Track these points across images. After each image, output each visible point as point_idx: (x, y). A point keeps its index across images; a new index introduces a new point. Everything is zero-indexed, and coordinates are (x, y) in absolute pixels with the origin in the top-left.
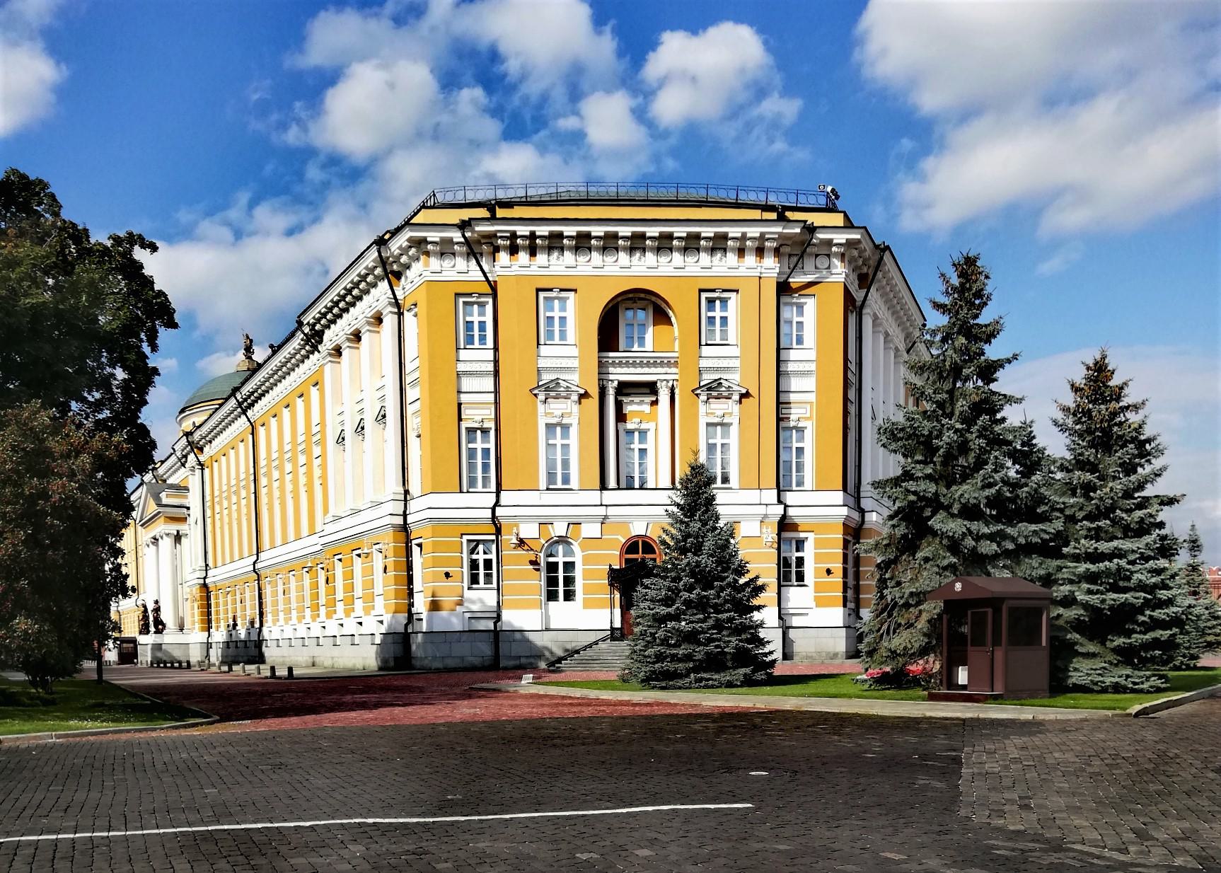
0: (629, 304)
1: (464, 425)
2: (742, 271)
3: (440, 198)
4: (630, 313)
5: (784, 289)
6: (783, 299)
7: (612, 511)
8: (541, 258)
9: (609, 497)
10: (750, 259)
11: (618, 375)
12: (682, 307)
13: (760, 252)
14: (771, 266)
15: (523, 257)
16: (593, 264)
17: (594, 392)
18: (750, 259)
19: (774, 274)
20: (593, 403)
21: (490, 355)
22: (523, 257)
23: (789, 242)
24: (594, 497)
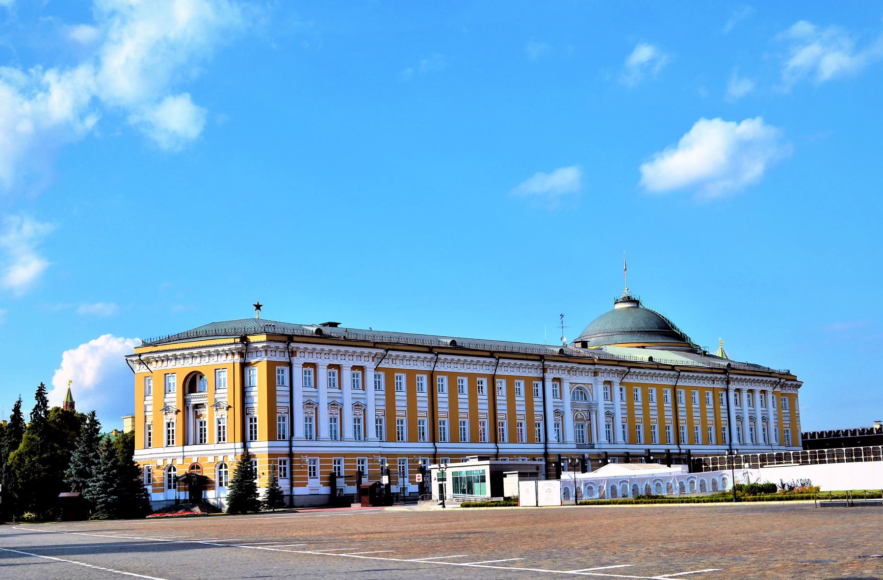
1: (147, 423)
5: (244, 366)
6: (247, 370)
7: (185, 454)
9: (186, 448)
10: (230, 357)
11: (194, 402)
12: (208, 377)
13: (233, 354)
16: (180, 364)
17: (181, 409)
18: (230, 357)
19: (239, 361)
20: (180, 414)
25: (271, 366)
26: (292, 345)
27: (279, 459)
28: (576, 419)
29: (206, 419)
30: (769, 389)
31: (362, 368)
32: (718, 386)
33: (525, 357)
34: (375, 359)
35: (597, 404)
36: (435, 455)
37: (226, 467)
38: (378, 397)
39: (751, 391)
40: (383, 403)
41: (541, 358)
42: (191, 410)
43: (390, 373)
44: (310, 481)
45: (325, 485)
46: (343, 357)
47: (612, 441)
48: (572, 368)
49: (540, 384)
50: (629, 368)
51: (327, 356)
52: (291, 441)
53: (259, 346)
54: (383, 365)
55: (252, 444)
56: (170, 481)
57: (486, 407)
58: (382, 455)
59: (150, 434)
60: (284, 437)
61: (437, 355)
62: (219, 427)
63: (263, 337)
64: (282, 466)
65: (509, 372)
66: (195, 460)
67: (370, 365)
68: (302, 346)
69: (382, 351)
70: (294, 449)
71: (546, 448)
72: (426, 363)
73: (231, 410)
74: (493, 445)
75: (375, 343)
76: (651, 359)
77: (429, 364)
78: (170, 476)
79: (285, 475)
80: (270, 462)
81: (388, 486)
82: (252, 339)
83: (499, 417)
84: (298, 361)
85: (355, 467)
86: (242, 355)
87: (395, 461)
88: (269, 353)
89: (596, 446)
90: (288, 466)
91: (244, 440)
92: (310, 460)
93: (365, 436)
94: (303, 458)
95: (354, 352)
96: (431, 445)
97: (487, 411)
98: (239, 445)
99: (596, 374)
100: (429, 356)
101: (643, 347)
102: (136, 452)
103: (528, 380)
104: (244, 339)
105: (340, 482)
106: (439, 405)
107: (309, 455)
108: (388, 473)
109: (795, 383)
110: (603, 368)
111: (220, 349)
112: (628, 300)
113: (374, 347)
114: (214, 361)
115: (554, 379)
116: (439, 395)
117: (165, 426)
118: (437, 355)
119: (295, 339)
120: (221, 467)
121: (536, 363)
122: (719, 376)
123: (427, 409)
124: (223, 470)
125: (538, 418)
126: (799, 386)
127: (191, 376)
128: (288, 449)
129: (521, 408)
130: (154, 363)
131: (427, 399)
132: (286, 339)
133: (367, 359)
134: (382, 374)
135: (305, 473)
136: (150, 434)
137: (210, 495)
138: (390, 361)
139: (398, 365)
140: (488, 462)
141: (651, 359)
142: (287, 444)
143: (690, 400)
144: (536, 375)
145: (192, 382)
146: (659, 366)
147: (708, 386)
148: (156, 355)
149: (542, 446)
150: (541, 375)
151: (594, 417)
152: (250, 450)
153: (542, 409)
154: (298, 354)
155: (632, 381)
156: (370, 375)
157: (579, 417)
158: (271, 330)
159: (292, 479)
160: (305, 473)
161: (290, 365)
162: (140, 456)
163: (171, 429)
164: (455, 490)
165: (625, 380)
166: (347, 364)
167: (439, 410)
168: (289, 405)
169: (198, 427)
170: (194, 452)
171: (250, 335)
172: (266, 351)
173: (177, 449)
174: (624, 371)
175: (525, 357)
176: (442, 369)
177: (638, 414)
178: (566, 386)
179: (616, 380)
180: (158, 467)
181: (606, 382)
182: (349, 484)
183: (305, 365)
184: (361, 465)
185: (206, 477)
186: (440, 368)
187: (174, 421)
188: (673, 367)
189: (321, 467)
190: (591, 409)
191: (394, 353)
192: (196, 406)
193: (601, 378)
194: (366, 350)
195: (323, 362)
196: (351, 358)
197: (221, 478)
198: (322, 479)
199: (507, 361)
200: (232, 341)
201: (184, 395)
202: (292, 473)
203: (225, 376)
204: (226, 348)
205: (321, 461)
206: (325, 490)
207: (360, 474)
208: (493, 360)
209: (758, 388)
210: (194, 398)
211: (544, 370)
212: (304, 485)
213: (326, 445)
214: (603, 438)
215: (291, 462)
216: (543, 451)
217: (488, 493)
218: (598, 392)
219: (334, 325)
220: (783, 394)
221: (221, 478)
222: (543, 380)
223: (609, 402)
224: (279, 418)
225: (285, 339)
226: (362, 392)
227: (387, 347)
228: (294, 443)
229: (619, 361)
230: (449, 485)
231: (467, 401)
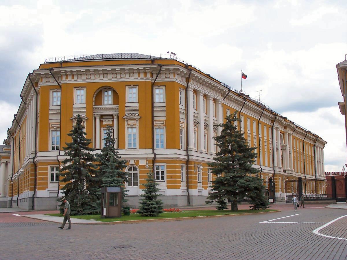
0: (105, 90)
2: (139, 80)
3: (48, 61)
4: (106, 93)
6: (154, 88)
8: (75, 78)
10: (142, 75)
13: (145, 73)
14: (148, 78)
15: (70, 78)
21: (59, 108)
22: (70, 78)
23: (155, 70)
32: (312, 143)
37: (135, 169)
42: (98, 121)
54: (224, 102)
86: (152, 74)
89: (286, 172)
98: (150, 151)
99: (285, 128)
111: (135, 67)
124: (133, 172)
128: (186, 157)
130: (64, 78)
150: (271, 124)
152: (157, 156)
172: (174, 73)
192: (102, 117)
202: (187, 178)
204: (141, 67)
215: (187, 168)
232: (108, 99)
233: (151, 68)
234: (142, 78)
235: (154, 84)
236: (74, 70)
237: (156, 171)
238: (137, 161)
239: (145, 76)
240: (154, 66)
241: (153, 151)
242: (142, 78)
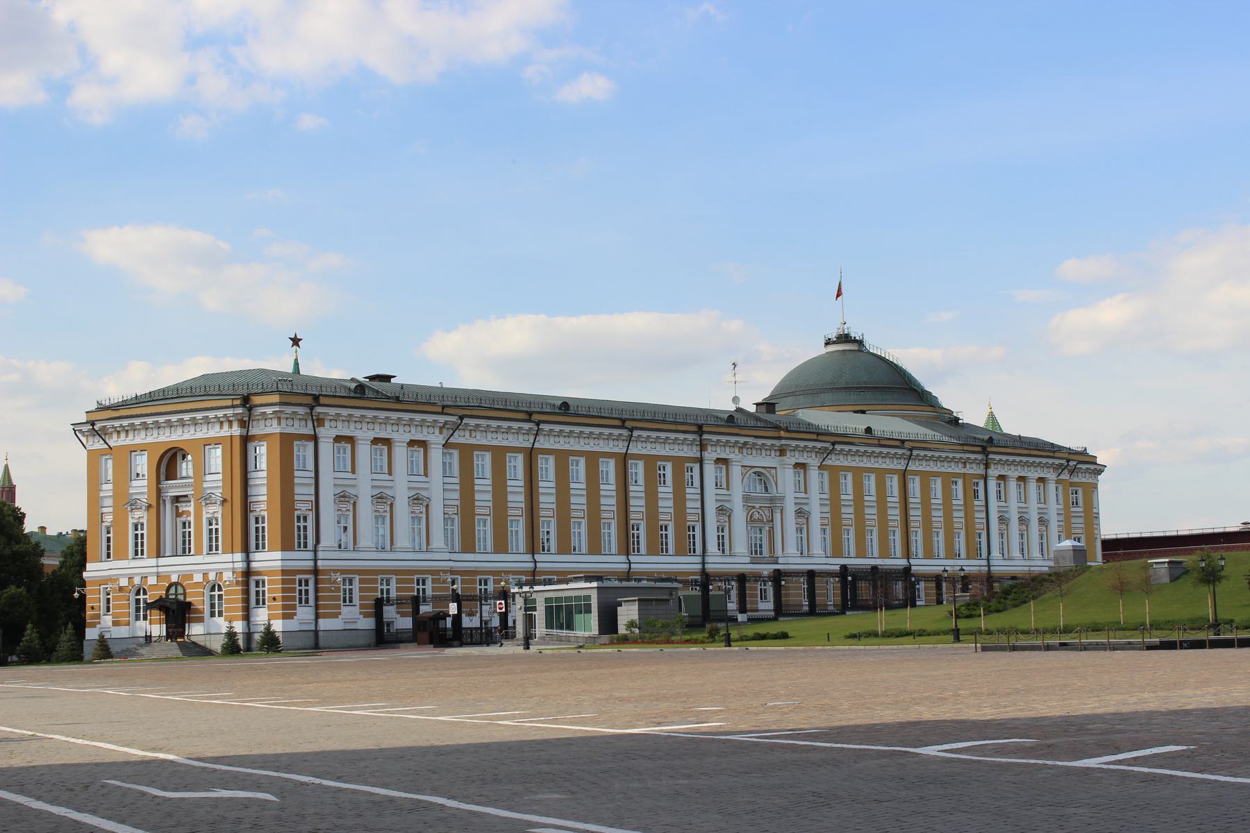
5: (246, 440)
6: (251, 446)
7: (160, 569)
9: (162, 561)
10: (226, 426)
14: (236, 431)
15: (123, 435)
17: (154, 504)
20: (154, 511)
22: (123, 435)
24: (153, 562)
25: (287, 442)
26: (319, 409)
27: (298, 577)
28: (751, 520)
29: (192, 519)
30: (1051, 475)
31: (423, 444)
32: (971, 471)
33: (673, 427)
34: (445, 431)
35: (782, 498)
36: (534, 572)
37: (220, 589)
38: (447, 487)
39: (1022, 479)
40: (456, 495)
41: (700, 426)
42: (168, 506)
43: (467, 452)
44: (344, 610)
45: (366, 615)
46: (395, 428)
47: (805, 553)
48: (746, 443)
49: (696, 467)
50: (833, 444)
51: (371, 426)
52: (315, 551)
53: (269, 410)
55: (256, 556)
56: (138, 610)
57: (613, 501)
58: (452, 572)
59: (109, 539)
60: (305, 546)
61: (538, 425)
62: (211, 530)
63: (275, 398)
64: (303, 588)
65: (649, 450)
66: (174, 579)
67: (436, 439)
68: (332, 411)
69: (454, 419)
70: (319, 563)
71: (703, 563)
72: (425, 430)
73: (228, 505)
74: (623, 558)
75: (443, 407)
76: (869, 430)
77: (526, 437)
78: (138, 601)
79: (307, 601)
80: (284, 582)
81: (457, 619)
82: (257, 400)
83: (632, 516)
84: (327, 433)
85: (412, 589)
86: (244, 424)
87: (474, 582)
88: (283, 422)
90: (311, 587)
91: (246, 550)
92: (344, 580)
93: (428, 544)
94: (333, 576)
95: (350, 415)
96: (528, 557)
97: (614, 508)
98: (239, 556)
100: (526, 426)
101: (863, 412)
102: (89, 566)
103: (678, 462)
104: (246, 400)
105: (390, 612)
106: (542, 499)
107: (343, 572)
108: (456, 598)
109: (1092, 467)
110: (794, 443)
111: (211, 414)
112: (845, 338)
113: (442, 413)
114: (202, 433)
115: (718, 461)
116: (541, 484)
117: (131, 528)
118: (538, 425)
119: (322, 400)
120: (213, 589)
121: (690, 437)
122: (973, 456)
123: (523, 505)
124: (216, 593)
125: (692, 518)
126: (1100, 472)
127: (169, 455)
128: (311, 563)
129: (666, 504)
130: (115, 435)
131: (522, 490)
132: (310, 399)
133: (431, 430)
134: (456, 453)
135: (338, 598)
136: (109, 539)
137: (195, 631)
138: (467, 433)
139: (480, 439)
140: (595, 584)
141: (869, 430)
142: (310, 555)
143: (653, 481)
144: (690, 454)
145: (169, 462)
146: (882, 442)
147: (957, 471)
148: (117, 424)
149: (699, 559)
150: (698, 455)
151: (777, 516)
152: (254, 565)
153: (698, 505)
154: (327, 423)
155: (837, 463)
156: (436, 455)
157: (756, 516)
158: (285, 388)
159: (317, 607)
160: (338, 598)
161: (315, 438)
162: (93, 570)
163: (139, 532)
164: (549, 625)
165: (828, 462)
166: (401, 436)
167: (541, 506)
168: (313, 498)
169: (180, 530)
170: (174, 566)
171: (256, 394)
172: (279, 419)
173: (147, 564)
174: (826, 448)
175: (673, 427)
176: (547, 446)
177: (848, 512)
178: (736, 471)
179: (813, 461)
180: (121, 589)
181: (798, 465)
182: (403, 615)
183: (338, 439)
184: (421, 587)
185: (190, 604)
186: (543, 443)
187: (145, 521)
188: (903, 441)
189: (361, 590)
190: (774, 503)
191: (472, 422)
192: (177, 499)
193: (791, 459)
194: (430, 418)
195: (364, 434)
196: (407, 428)
197: (212, 606)
198: (362, 606)
199: (645, 434)
200: (229, 403)
201: (158, 482)
202: (317, 599)
203: (216, 457)
204: (220, 413)
205: (361, 581)
206: (368, 623)
207: (416, 601)
208: (625, 432)
209: (1033, 474)
210: (173, 488)
211: (702, 447)
212: (336, 615)
213: (368, 558)
214: (792, 549)
215: (316, 582)
216: (700, 566)
217: (595, 630)
218: (786, 481)
219: (387, 378)
220: (1072, 484)
221: (212, 606)
222: (701, 461)
223: (803, 495)
224: (299, 518)
225: (309, 400)
226: (387, 477)
227: (461, 412)
228: (320, 555)
229: (818, 434)
230: (540, 615)
231: (584, 492)
232: (186, 468)
233: (235, 415)
234: (225, 432)
235: (246, 440)
236: (125, 423)
237: (253, 589)
238: (219, 574)
239: (231, 426)
240: (240, 410)
241: (248, 556)
242: (225, 432)
